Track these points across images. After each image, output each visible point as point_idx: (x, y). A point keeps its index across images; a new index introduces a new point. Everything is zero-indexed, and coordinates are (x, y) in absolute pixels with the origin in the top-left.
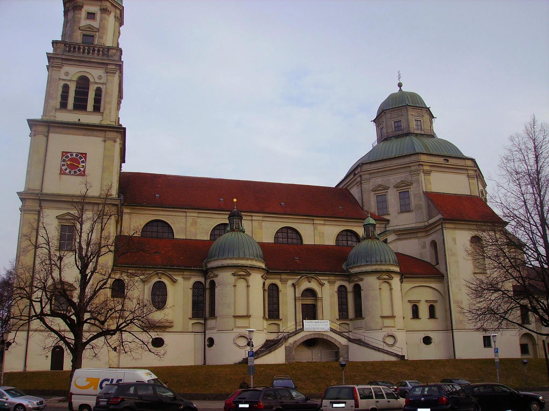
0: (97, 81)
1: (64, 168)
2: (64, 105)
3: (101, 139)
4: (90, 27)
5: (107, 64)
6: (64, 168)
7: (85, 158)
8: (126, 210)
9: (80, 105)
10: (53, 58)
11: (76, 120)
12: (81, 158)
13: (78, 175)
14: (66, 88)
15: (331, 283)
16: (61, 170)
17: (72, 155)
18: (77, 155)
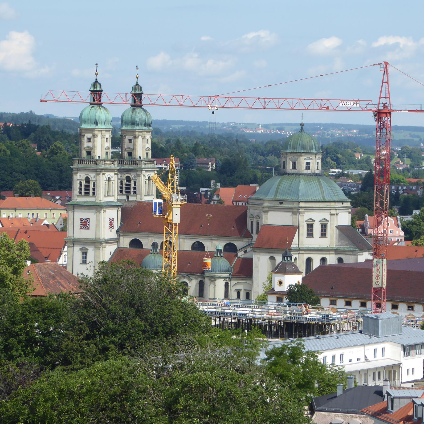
0: (93, 179)
1: (81, 226)
2: (80, 193)
4: (88, 147)
6: (81, 226)
8: (121, 234)
11: (86, 200)
15: (196, 279)
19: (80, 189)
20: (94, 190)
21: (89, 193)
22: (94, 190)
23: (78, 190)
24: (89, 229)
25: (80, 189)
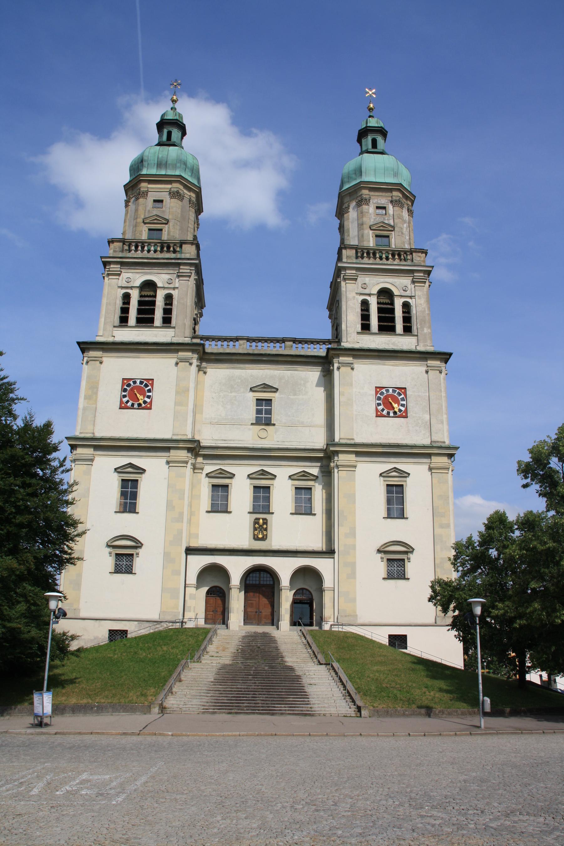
1: (125, 400)
2: (124, 320)
3: (174, 361)
5: (179, 265)
6: (125, 400)
7: (152, 385)
9: (145, 318)
10: (110, 263)
12: (146, 386)
13: (143, 408)
14: (127, 298)
16: (121, 402)
17: (135, 382)
18: (141, 383)
19: (125, 310)
20: (168, 312)
21: (152, 321)
22: (168, 312)
23: (118, 313)
24: (150, 408)
25: (125, 310)
